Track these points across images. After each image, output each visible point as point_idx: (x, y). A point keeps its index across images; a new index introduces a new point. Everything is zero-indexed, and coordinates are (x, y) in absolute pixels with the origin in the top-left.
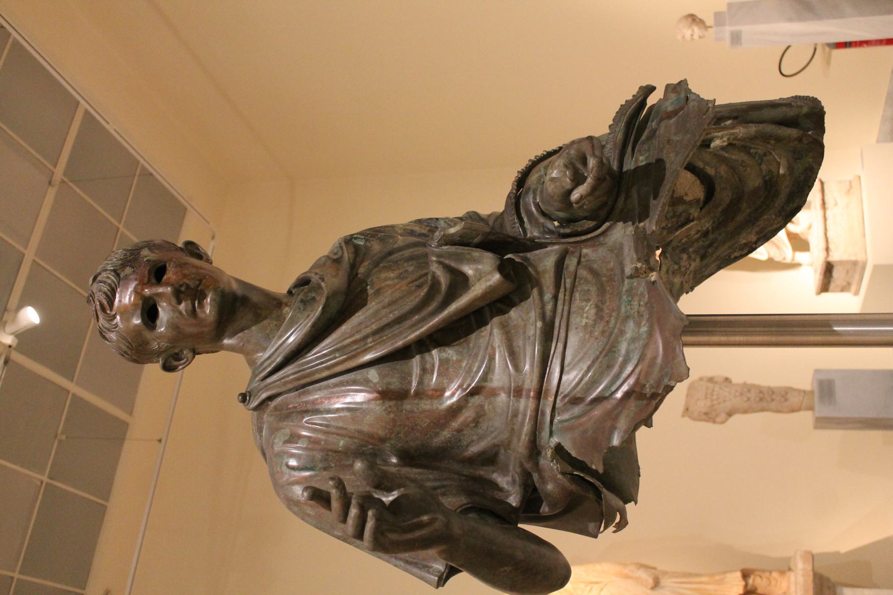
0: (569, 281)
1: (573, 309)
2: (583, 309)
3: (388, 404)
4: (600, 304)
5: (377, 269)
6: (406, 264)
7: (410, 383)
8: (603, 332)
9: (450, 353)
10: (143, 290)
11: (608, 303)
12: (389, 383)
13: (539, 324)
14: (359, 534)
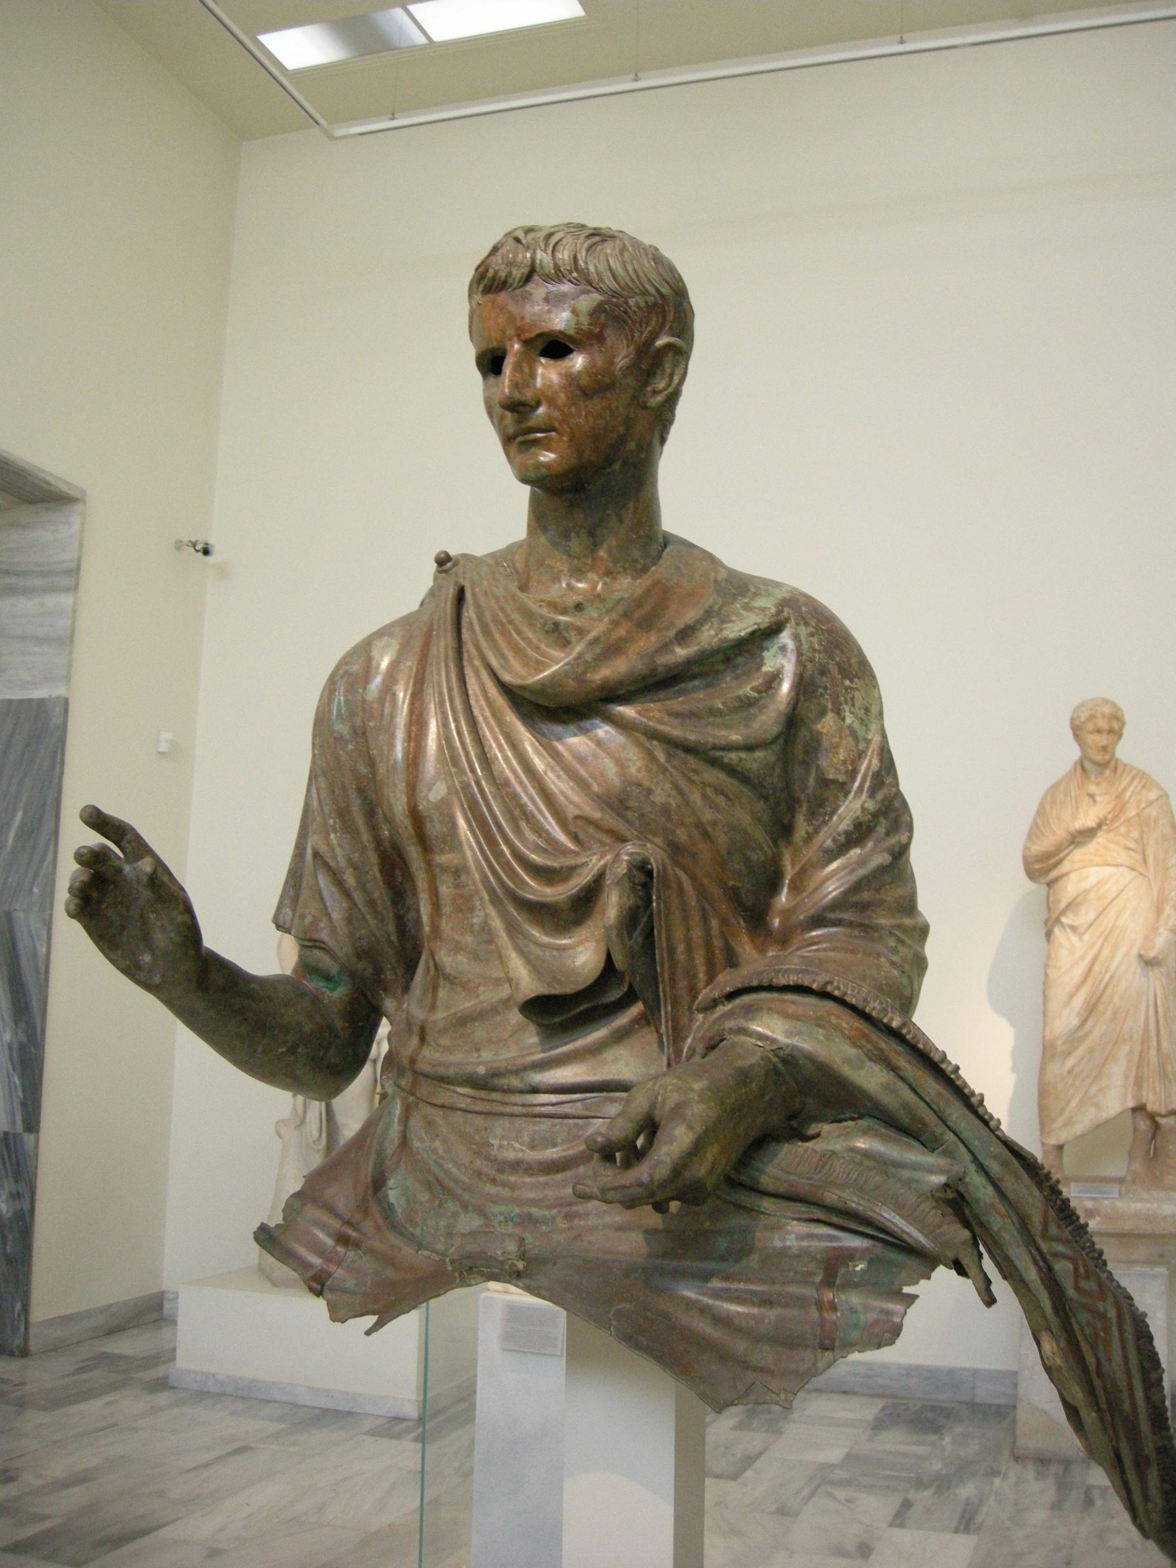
0: (578, 1108)
1: (518, 1122)
2: (516, 1139)
3: (408, 822)
4: (524, 1166)
5: (642, 738)
6: (668, 786)
7: (442, 852)
8: (479, 1174)
10: (510, 339)
11: (528, 1180)
12: (432, 821)
13: (481, 1070)
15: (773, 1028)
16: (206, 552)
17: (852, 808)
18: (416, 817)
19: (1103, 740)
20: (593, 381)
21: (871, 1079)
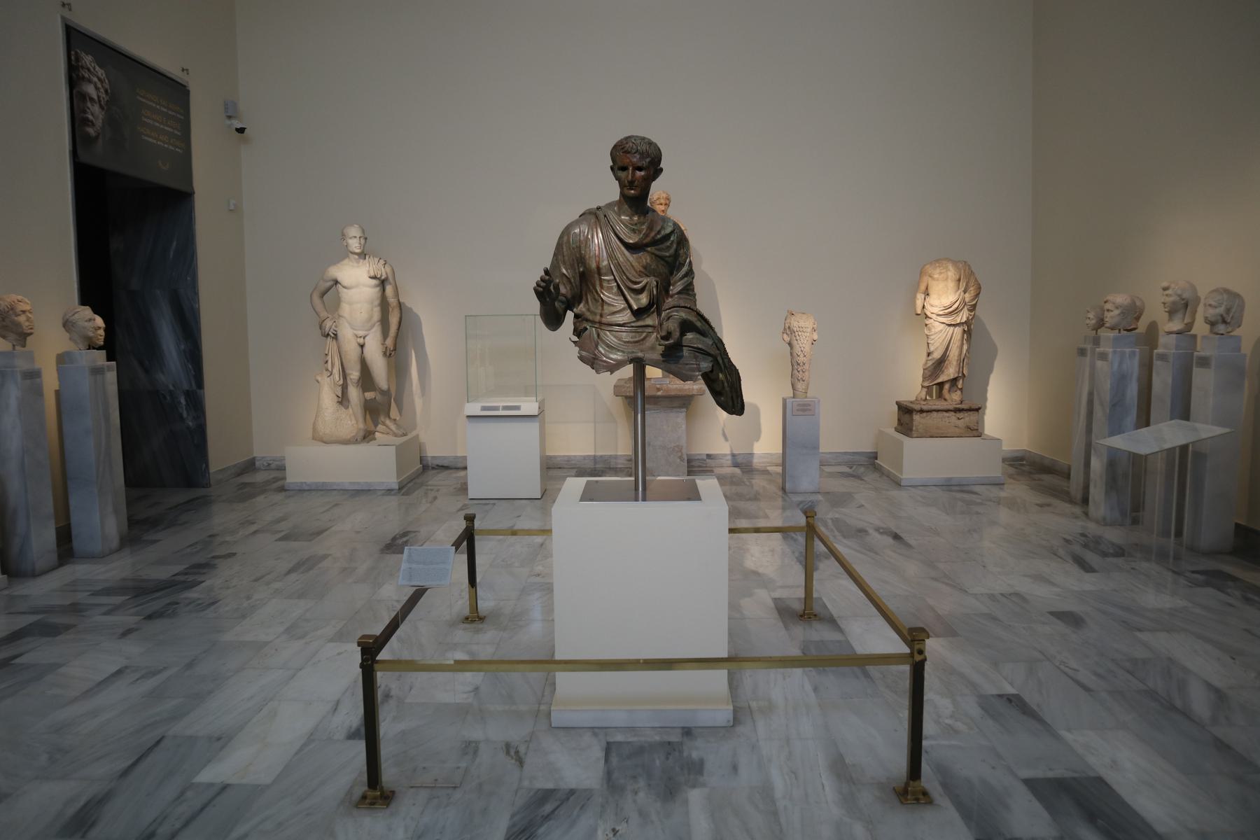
9: (615, 290)
14: (538, 285)
15: (683, 314)
16: (64, 5)
17: (685, 269)
18: (598, 268)
19: (662, 208)
20: (637, 166)
21: (699, 324)
